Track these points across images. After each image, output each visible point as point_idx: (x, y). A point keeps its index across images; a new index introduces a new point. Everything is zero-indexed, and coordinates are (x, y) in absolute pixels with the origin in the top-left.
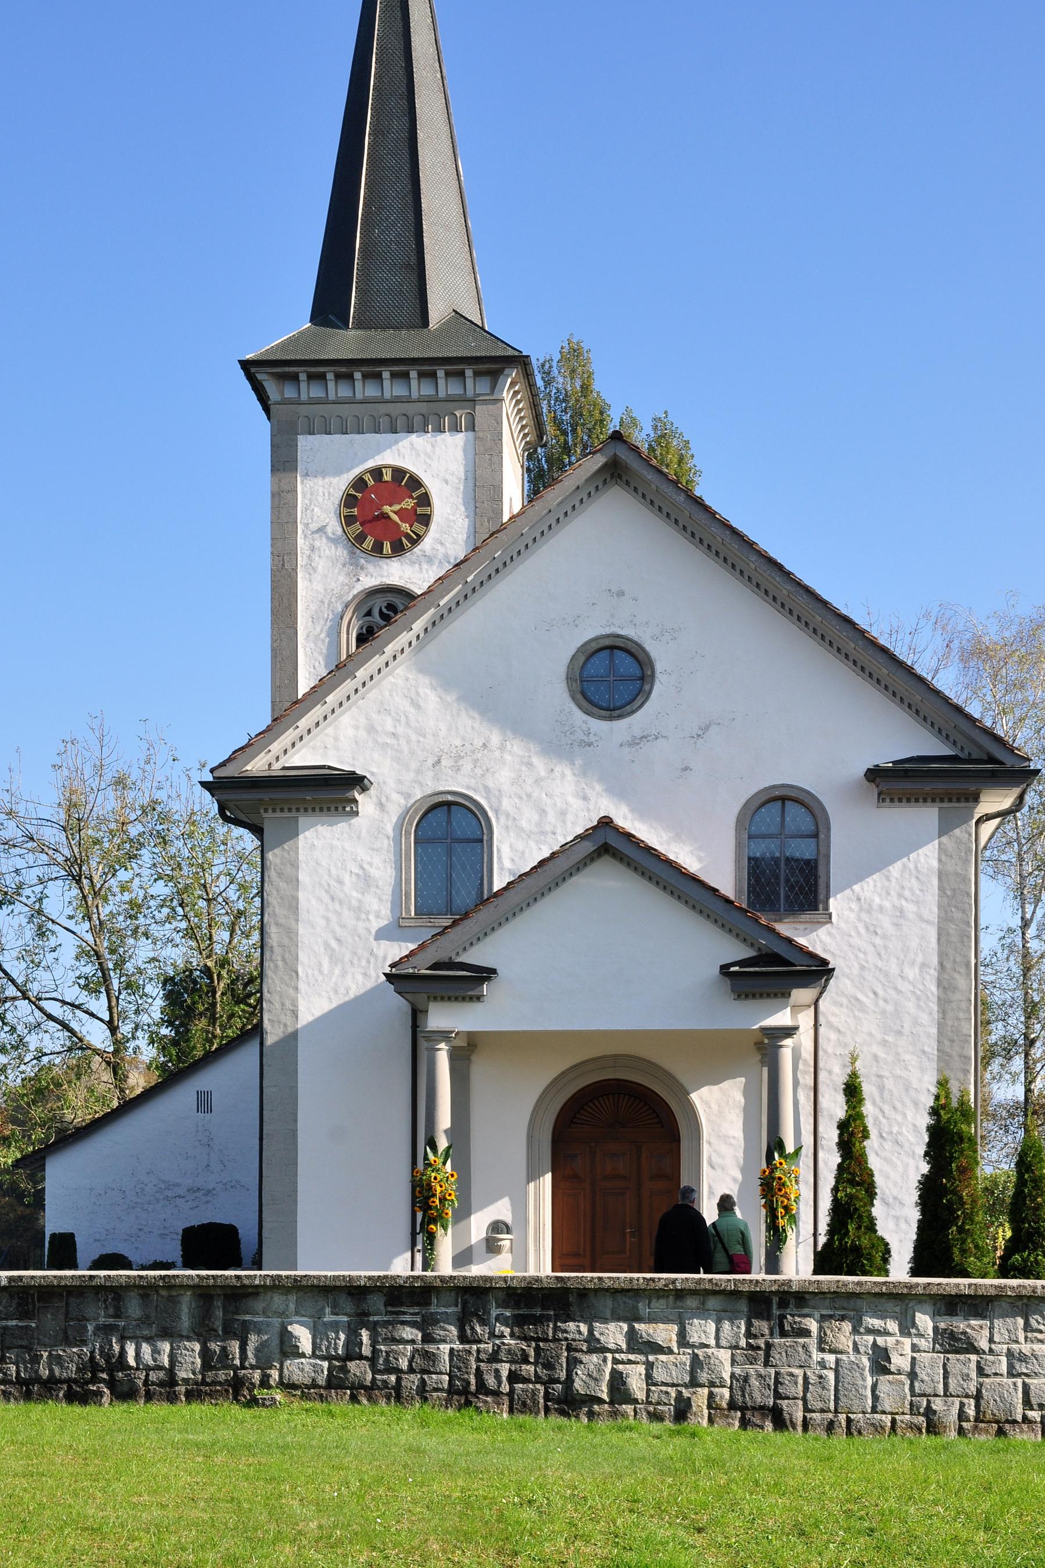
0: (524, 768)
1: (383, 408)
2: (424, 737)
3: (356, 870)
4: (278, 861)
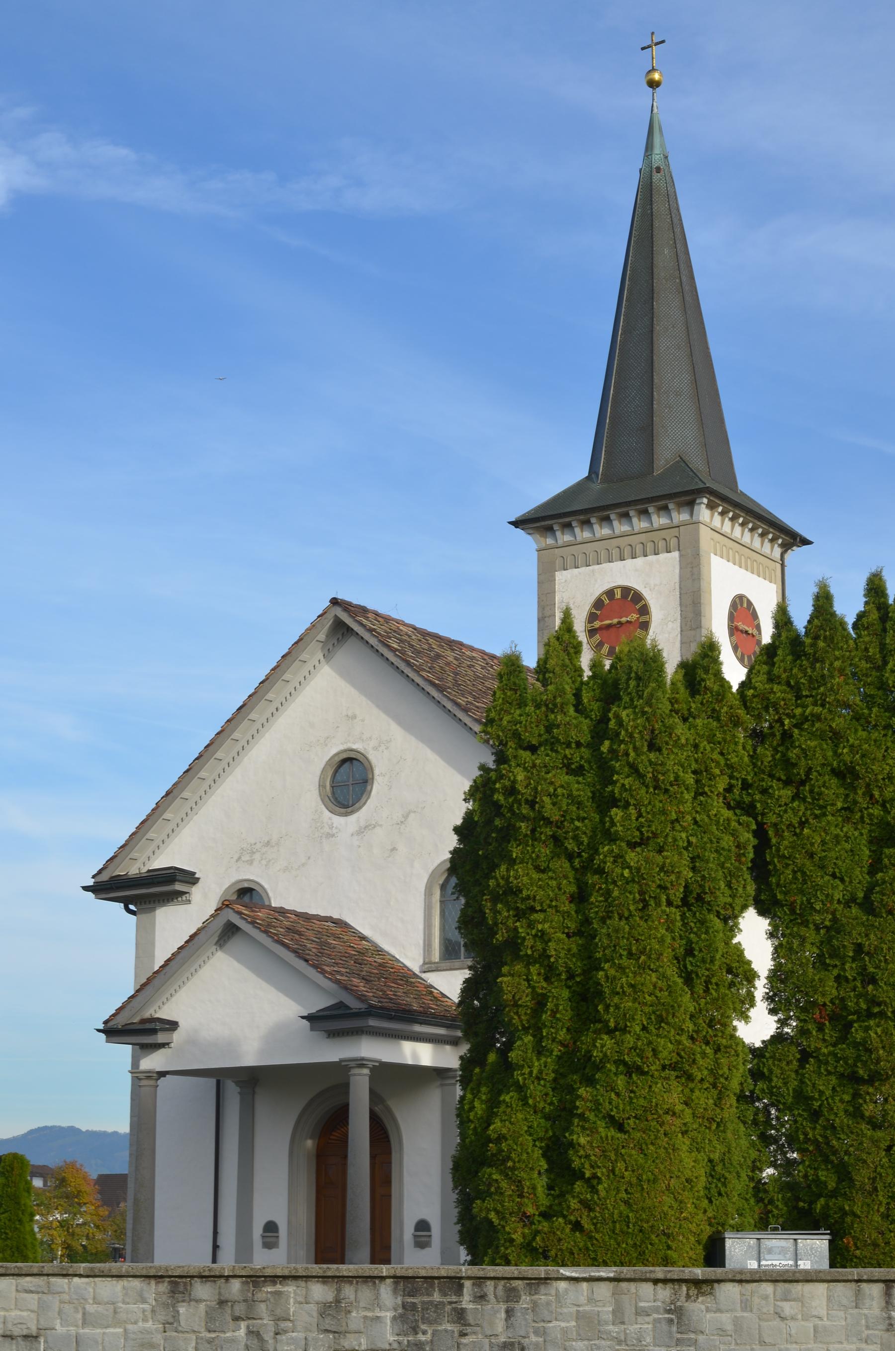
1: (615, 542)
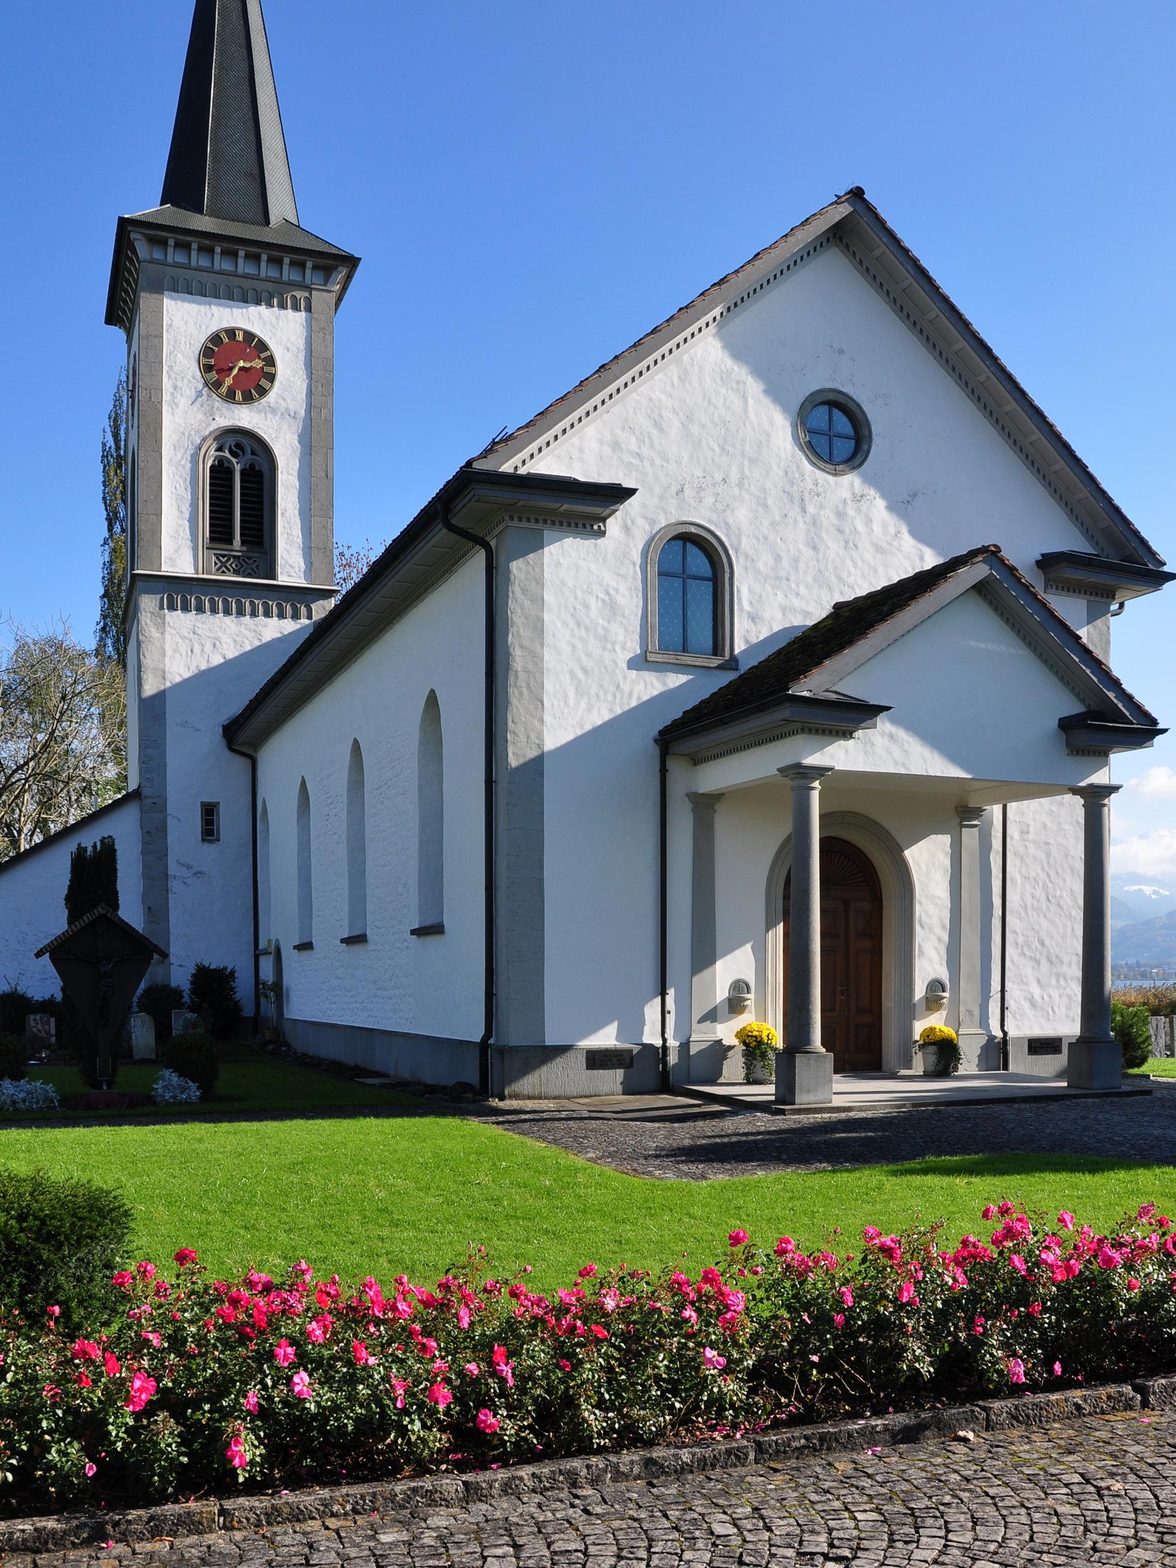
0: (760, 509)
1: (236, 281)
2: (668, 462)
3: (602, 596)
4: (523, 577)
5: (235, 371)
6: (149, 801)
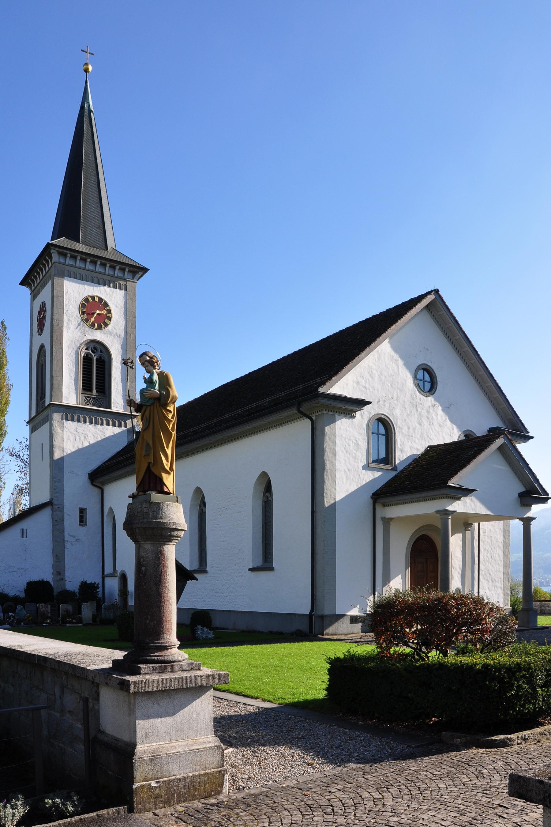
1: (95, 275)
5: (95, 315)
6: (57, 506)
